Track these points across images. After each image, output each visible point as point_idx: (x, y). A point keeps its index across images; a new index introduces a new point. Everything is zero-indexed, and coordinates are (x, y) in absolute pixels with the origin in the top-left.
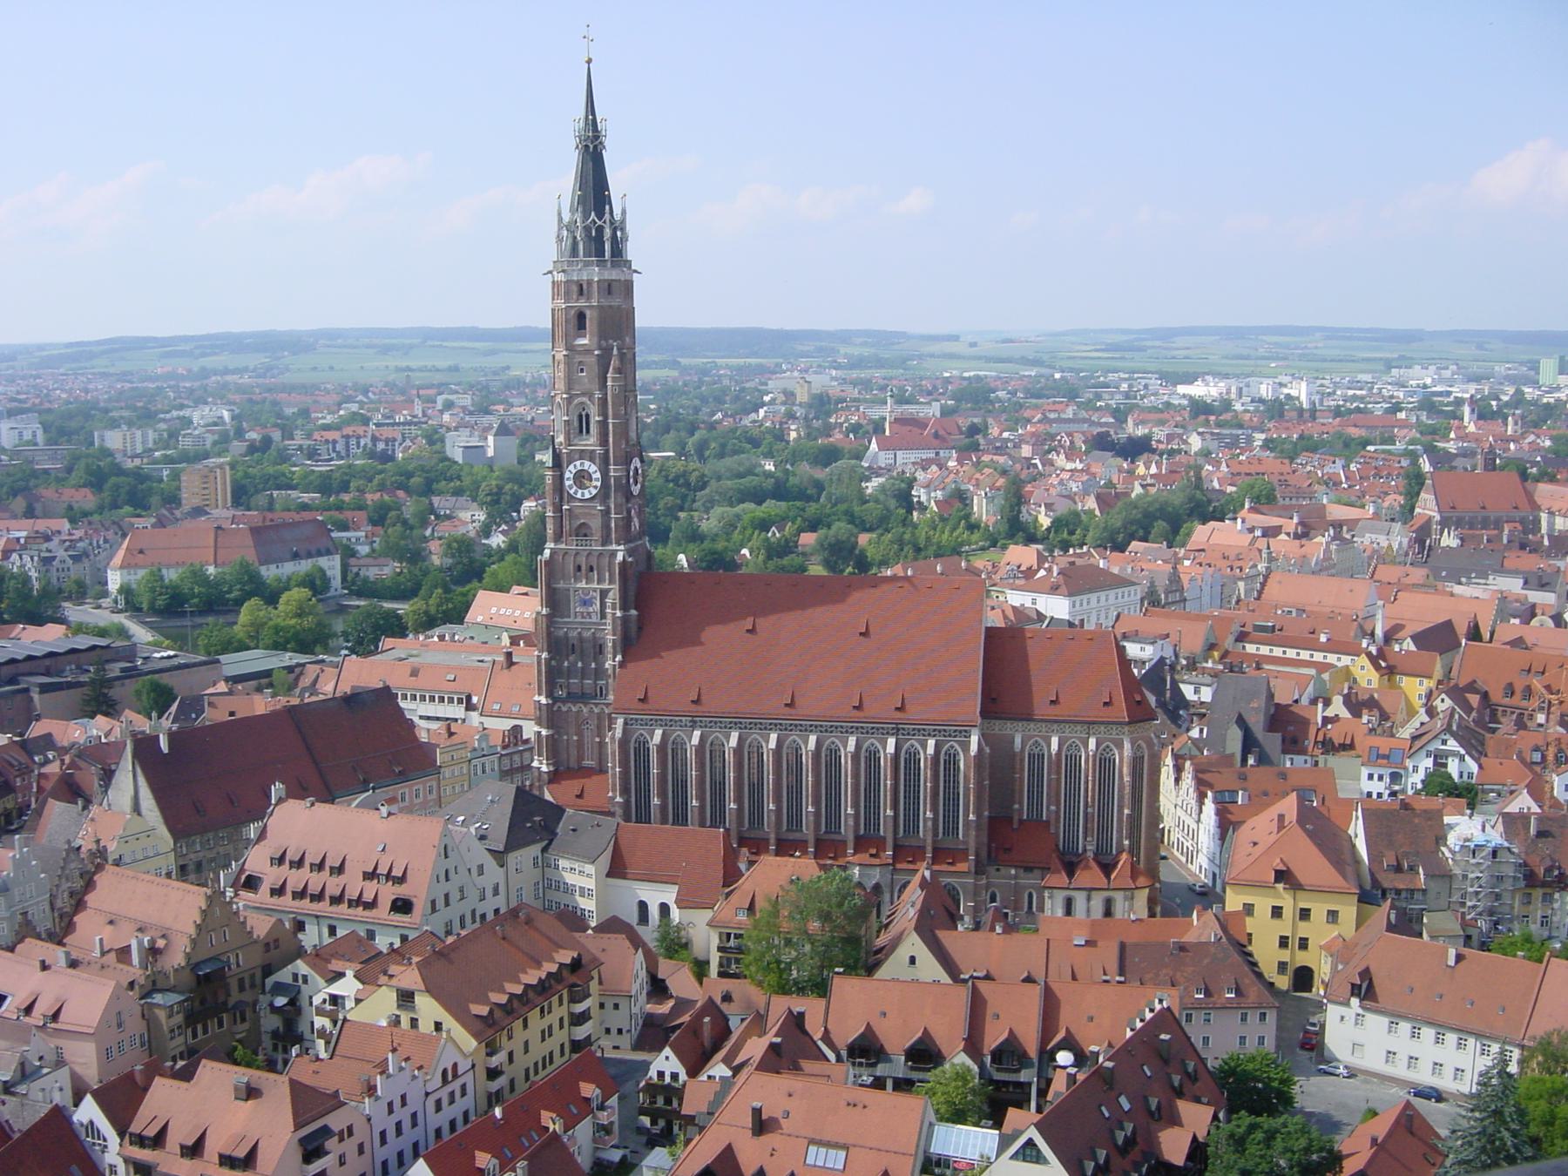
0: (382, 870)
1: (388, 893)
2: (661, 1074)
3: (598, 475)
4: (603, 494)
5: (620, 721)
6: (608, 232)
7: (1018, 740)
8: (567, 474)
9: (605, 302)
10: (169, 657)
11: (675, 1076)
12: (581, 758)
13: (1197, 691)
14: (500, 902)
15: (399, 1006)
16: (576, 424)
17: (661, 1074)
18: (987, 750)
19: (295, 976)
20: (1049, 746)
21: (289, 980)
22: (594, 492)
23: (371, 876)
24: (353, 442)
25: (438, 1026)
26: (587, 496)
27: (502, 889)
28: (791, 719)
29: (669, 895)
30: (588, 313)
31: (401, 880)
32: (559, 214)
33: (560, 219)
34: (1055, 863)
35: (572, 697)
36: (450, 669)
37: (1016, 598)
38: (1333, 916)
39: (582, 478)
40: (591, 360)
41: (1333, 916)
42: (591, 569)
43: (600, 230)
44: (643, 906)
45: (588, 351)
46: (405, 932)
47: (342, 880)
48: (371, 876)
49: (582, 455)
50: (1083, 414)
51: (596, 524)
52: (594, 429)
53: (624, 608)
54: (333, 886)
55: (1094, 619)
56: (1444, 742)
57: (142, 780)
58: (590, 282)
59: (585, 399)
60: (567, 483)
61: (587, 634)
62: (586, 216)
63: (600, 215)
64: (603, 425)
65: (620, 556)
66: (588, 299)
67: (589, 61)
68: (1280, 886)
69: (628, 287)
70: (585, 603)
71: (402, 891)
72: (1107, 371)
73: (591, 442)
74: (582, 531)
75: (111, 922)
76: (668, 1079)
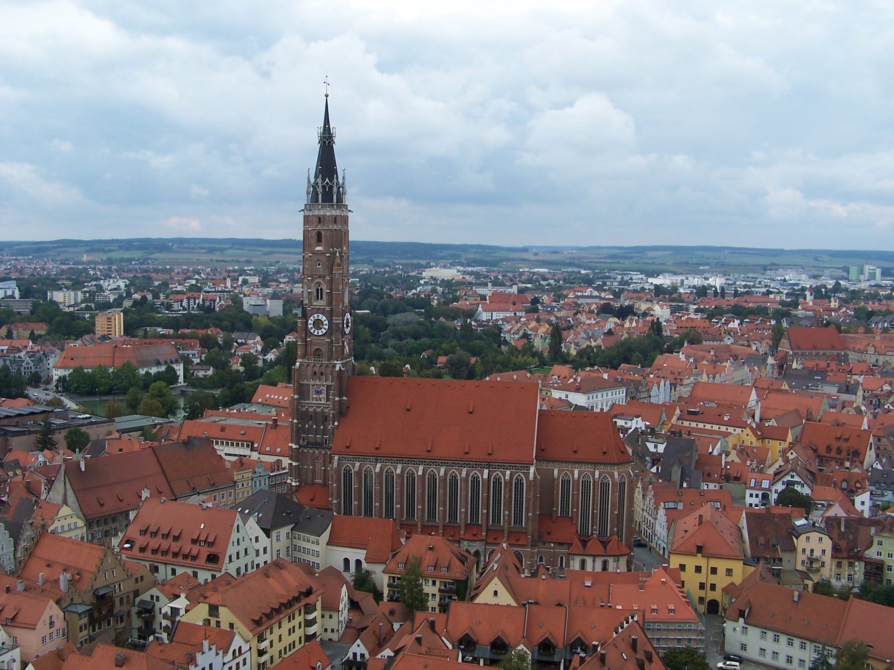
0: (203, 538)
1: (205, 551)
2: (355, 654)
3: (326, 322)
5: (336, 457)
6: (335, 190)
7: (556, 472)
8: (310, 322)
9: (331, 227)
10: (86, 418)
11: (362, 655)
12: (314, 478)
13: (656, 447)
14: (267, 557)
15: (210, 615)
17: (355, 654)
18: (539, 477)
19: (152, 596)
20: (573, 476)
21: (149, 599)
22: (324, 331)
23: (194, 542)
24: (192, 301)
25: (232, 626)
27: (269, 550)
28: (429, 459)
29: (361, 554)
30: (323, 233)
31: (211, 544)
32: (309, 178)
33: (309, 182)
34: (577, 542)
35: (310, 445)
36: (243, 427)
37: (557, 394)
38: (729, 572)
39: (318, 324)
40: (324, 259)
41: (729, 572)
42: (322, 374)
43: (331, 188)
44: (347, 561)
45: (322, 253)
46: (214, 573)
47: (179, 543)
48: (194, 542)
49: (318, 311)
50: (596, 293)
51: (324, 349)
52: (324, 297)
53: (340, 396)
54: (175, 547)
55: (599, 407)
56: (792, 477)
57: (68, 486)
58: (324, 216)
59: (320, 280)
60: (310, 326)
61: (319, 410)
62: (323, 180)
63: (331, 180)
65: (337, 368)
67: (327, 96)
68: (699, 555)
69: (345, 220)
70: (318, 393)
71: (213, 550)
72: (610, 270)
73: (322, 303)
74: (318, 353)
75: (48, 566)
76: (359, 659)
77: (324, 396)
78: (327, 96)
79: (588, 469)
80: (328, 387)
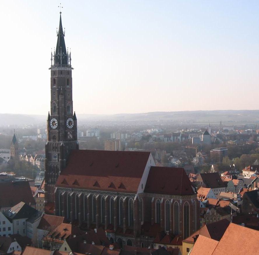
4: (58, 128)
7: (153, 199)
9: (59, 76)
14: (11, 232)
16: (53, 109)
26: (55, 128)
27: (12, 228)
30: (56, 79)
35: (52, 183)
51: (57, 135)
58: (56, 71)
60: (51, 125)
61: (55, 166)
64: (59, 108)
65: (61, 145)
66: (56, 75)
67: (61, 13)
69: (69, 73)
77: (57, 159)
78: (61, 13)
79: (167, 197)
80: (58, 154)
